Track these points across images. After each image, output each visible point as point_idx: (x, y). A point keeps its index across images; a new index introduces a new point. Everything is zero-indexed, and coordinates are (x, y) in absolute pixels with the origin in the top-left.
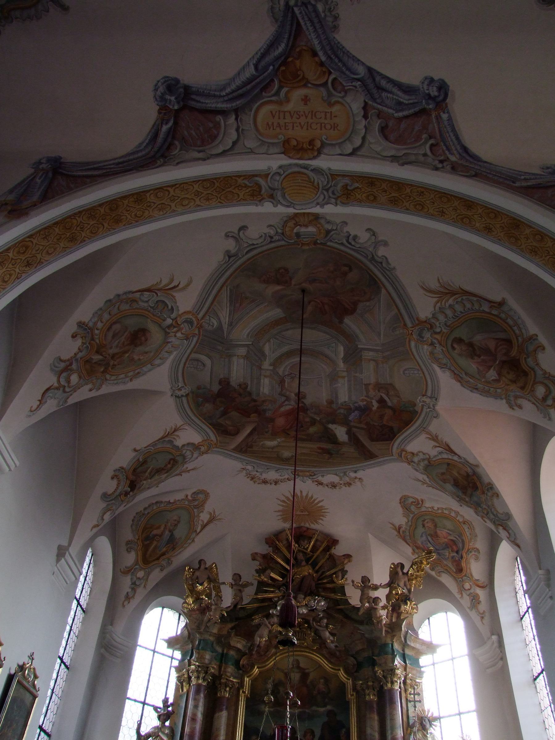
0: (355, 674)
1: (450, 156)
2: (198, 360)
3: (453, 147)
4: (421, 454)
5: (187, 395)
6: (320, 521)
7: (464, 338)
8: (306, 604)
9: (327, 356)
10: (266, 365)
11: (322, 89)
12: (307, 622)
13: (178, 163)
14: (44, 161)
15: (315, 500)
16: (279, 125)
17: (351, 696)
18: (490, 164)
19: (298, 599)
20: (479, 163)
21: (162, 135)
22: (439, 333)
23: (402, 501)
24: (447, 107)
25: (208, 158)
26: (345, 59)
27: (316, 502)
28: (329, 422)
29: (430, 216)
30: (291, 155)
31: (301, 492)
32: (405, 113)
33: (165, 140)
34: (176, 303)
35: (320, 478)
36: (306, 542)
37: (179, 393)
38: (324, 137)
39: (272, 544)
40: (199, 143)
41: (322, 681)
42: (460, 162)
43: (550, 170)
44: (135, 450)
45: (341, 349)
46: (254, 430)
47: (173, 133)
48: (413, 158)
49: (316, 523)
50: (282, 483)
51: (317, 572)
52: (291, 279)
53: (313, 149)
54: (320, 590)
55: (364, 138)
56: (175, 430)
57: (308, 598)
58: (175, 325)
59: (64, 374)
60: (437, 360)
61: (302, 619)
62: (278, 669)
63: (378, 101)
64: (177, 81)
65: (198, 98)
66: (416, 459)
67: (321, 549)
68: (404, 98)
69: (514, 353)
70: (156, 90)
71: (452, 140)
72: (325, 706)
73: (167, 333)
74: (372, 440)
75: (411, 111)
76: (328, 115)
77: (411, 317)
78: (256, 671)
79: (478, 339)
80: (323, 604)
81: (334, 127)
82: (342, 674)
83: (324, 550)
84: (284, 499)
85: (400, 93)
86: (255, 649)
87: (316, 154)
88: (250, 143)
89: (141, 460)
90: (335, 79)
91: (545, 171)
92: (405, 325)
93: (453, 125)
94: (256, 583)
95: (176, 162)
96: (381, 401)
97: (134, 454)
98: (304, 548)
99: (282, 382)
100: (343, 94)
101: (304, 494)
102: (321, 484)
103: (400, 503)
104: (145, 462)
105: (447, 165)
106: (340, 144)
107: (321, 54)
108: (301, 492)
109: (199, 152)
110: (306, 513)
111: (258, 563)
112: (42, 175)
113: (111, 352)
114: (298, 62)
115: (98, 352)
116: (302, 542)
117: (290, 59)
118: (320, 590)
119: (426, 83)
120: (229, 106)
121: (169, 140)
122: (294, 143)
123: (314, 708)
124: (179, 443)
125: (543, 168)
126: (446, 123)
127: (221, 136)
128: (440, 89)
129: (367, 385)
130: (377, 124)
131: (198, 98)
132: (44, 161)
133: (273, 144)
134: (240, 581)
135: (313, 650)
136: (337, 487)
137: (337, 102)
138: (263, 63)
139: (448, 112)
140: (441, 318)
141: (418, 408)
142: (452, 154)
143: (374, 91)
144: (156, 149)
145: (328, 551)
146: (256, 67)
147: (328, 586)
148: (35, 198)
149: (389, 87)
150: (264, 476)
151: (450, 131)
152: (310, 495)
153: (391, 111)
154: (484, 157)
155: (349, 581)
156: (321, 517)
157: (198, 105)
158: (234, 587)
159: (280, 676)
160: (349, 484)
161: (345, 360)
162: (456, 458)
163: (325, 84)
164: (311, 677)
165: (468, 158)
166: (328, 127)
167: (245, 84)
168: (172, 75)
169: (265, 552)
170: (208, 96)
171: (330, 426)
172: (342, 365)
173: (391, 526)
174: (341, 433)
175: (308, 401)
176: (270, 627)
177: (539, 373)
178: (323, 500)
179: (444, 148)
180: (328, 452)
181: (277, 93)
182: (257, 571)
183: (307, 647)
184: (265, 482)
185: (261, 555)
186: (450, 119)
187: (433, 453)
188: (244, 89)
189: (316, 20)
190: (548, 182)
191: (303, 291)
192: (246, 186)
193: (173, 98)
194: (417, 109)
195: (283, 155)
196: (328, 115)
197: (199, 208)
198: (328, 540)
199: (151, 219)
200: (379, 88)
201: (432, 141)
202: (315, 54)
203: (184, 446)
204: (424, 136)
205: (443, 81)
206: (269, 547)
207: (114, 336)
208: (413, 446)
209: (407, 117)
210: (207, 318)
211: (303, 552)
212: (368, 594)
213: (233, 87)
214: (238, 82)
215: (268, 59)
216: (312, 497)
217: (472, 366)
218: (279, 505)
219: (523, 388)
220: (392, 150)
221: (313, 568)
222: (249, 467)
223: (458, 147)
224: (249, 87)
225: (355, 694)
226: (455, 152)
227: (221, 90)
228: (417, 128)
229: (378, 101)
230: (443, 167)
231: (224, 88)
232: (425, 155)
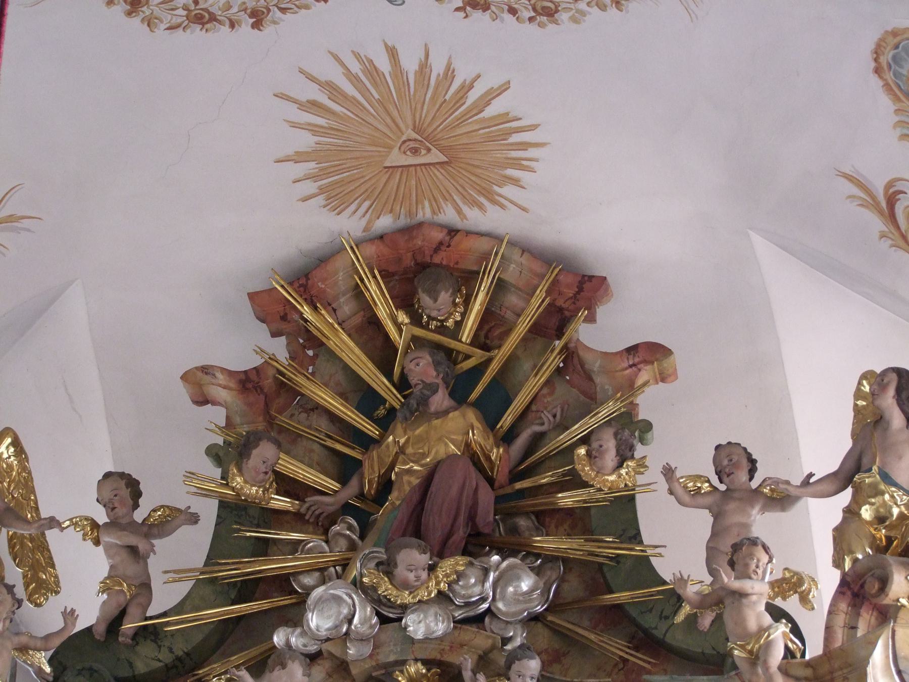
6: (508, 191)
8: (440, 593)
15: (467, 87)
19: (401, 571)
23: (883, 60)
27: (473, 96)
31: (392, 53)
36: (444, 297)
39: (284, 318)
49: (494, 202)
50: (288, 16)
51: (508, 438)
54: (523, 523)
57: (448, 566)
61: (426, 663)
67: (522, 328)
80: (525, 585)
83: (536, 330)
94: (209, 510)
98: (441, 329)
101: (410, 64)
103: (878, 71)
108: (392, 53)
110: (436, 156)
111: (218, 415)
116: (425, 299)
118: (523, 523)
134: (136, 506)
136: (564, 16)
145: (560, 334)
147: (567, 499)
152: (438, 66)
155: (654, 474)
156: (510, 172)
158: (106, 538)
169: (246, 361)
173: (856, 191)
178: (505, 87)
182: (215, 454)
185: (230, 373)
198: (555, 282)
206: (274, 334)
211: (437, 347)
212: (746, 526)
216: (449, 73)
218: (295, 125)
221: (491, 422)
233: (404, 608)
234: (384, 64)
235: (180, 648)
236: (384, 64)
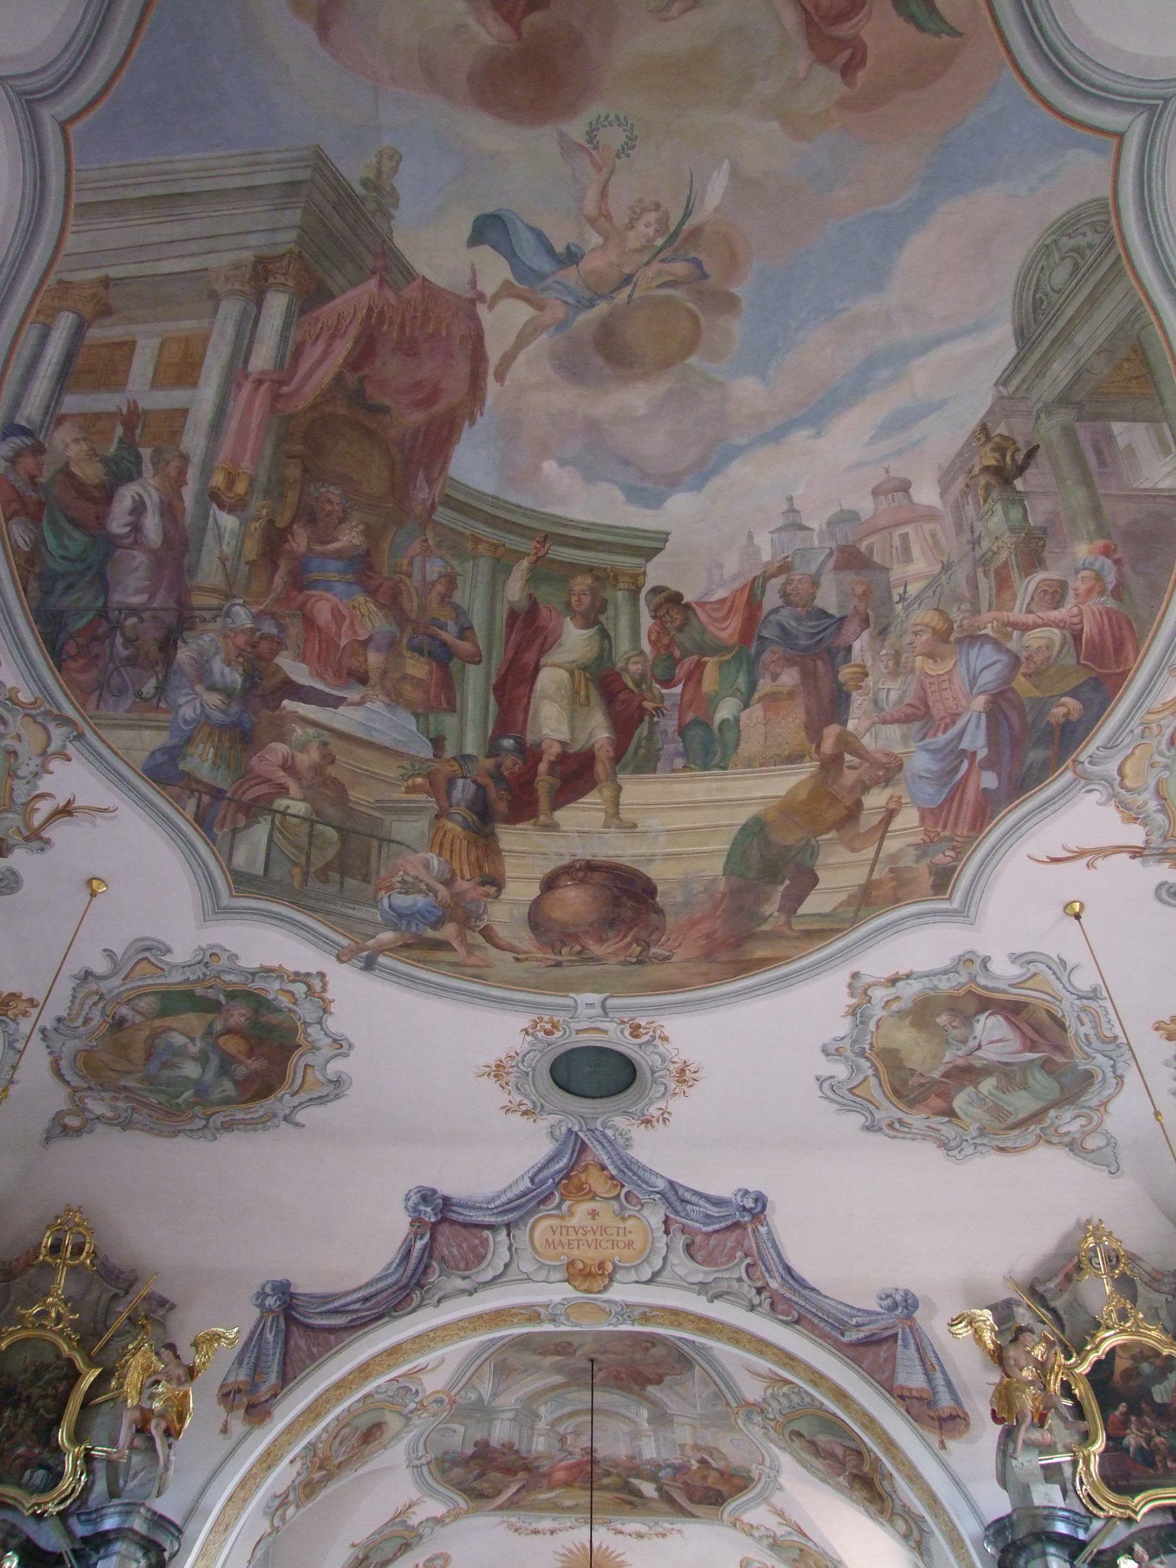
2: (447, 1429)
4: (762, 1529)
5: (428, 1463)
7: (804, 1432)
9: (623, 1416)
10: (541, 1425)
11: (613, 1202)
13: (439, 1301)
14: (268, 1290)
16: (561, 1243)
18: (819, 1294)
20: (805, 1292)
21: (416, 1253)
22: (772, 1420)
25: (476, 1290)
26: (641, 1173)
29: (749, 1351)
30: (576, 1284)
32: (717, 1227)
33: (420, 1260)
34: (422, 1384)
35: (619, 1527)
37: (418, 1463)
38: (616, 1259)
40: (462, 1265)
42: (782, 1291)
43: (889, 1301)
44: (353, 1545)
45: (645, 1413)
46: (523, 1487)
47: (430, 1249)
48: (724, 1286)
52: (575, 1351)
53: (603, 1275)
55: (665, 1259)
56: (410, 1506)
58: (422, 1406)
59: (279, 1513)
60: (772, 1441)
63: (683, 1214)
64: (434, 1192)
65: (460, 1210)
66: (756, 1533)
68: (713, 1211)
69: (866, 1468)
70: (407, 1199)
73: (408, 1419)
75: (723, 1225)
76: (621, 1231)
77: (735, 1398)
79: (822, 1439)
81: (629, 1245)
84: (563, 1551)
85: (707, 1205)
87: (607, 1281)
88: (527, 1266)
89: (360, 1556)
90: (629, 1192)
91: (884, 1303)
92: (728, 1404)
95: (436, 1298)
96: (702, 1462)
97: (352, 1550)
99: (563, 1439)
100: (639, 1207)
102: (621, 1532)
104: (366, 1557)
106: (636, 1267)
107: (611, 1168)
109: (464, 1278)
112: (272, 1321)
113: (337, 1462)
114: (583, 1177)
115: (321, 1468)
117: (573, 1173)
119: (740, 1194)
120: (499, 1219)
121: (425, 1260)
122: (580, 1265)
124: (414, 1521)
125: (881, 1299)
126: (765, 1237)
127: (489, 1256)
128: (756, 1200)
129: (682, 1446)
130: (680, 1241)
131: (460, 1210)
132: (268, 1290)
133: (555, 1267)
137: (631, 1216)
138: (541, 1176)
139: (767, 1225)
140: (774, 1404)
141: (755, 1474)
142: (772, 1277)
143: (677, 1204)
144: (409, 1273)
146: (532, 1180)
148: (273, 1378)
149: (695, 1199)
150: (534, 1526)
151: (769, 1245)
152: (604, 1546)
153: (697, 1225)
154: (811, 1280)
157: (461, 1219)
160: (664, 1535)
161: (649, 1421)
162: (810, 1544)
163: (617, 1197)
165: (791, 1282)
166: (621, 1245)
167: (518, 1197)
168: (429, 1184)
170: (474, 1208)
171: (632, 1480)
172: (646, 1425)
174: (648, 1489)
175: (598, 1455)
177: (897, 1502)
179: (763, 1269)
180: (631, 1503)
181: (559, 1207)
184: (535, 1532)
186: (769, 1232)
187: (780, 1531)
188: (518, 1202)
189: (604, 1141)
190: (886, 1329)
191: (592, 1361)
192: (522, 1314)
193: (429, 1209)
194: (729, 1222)
195: (567, 1284)
196: (621, 1231)
197: (462, 1338)
199: (405, 1361)
200: (683, 1201)
201: (749, 1260)
202: (603, 1168)
203: (421, 1523)
204: (739, 1254)
205: (760, 1193)
207: (341, 1443)
208: (750, 1517)
209: (716, 1231)
210: (463, 1393)
213: (504, 1199)
214: (510, 1195)
215: (546, 1173)
216: (607, 1548)
217: (818, 1464)
219: (881, 1513)
220: (698, 1273)
222: (513, 1520)
223: (780, 1268)
224: (523, 1200)
226: (776, 1274)
227: (489, 1203)
228: (729, 1244)
229: (683, 1214)
231: (493, 1200)
232: (740, 1280)
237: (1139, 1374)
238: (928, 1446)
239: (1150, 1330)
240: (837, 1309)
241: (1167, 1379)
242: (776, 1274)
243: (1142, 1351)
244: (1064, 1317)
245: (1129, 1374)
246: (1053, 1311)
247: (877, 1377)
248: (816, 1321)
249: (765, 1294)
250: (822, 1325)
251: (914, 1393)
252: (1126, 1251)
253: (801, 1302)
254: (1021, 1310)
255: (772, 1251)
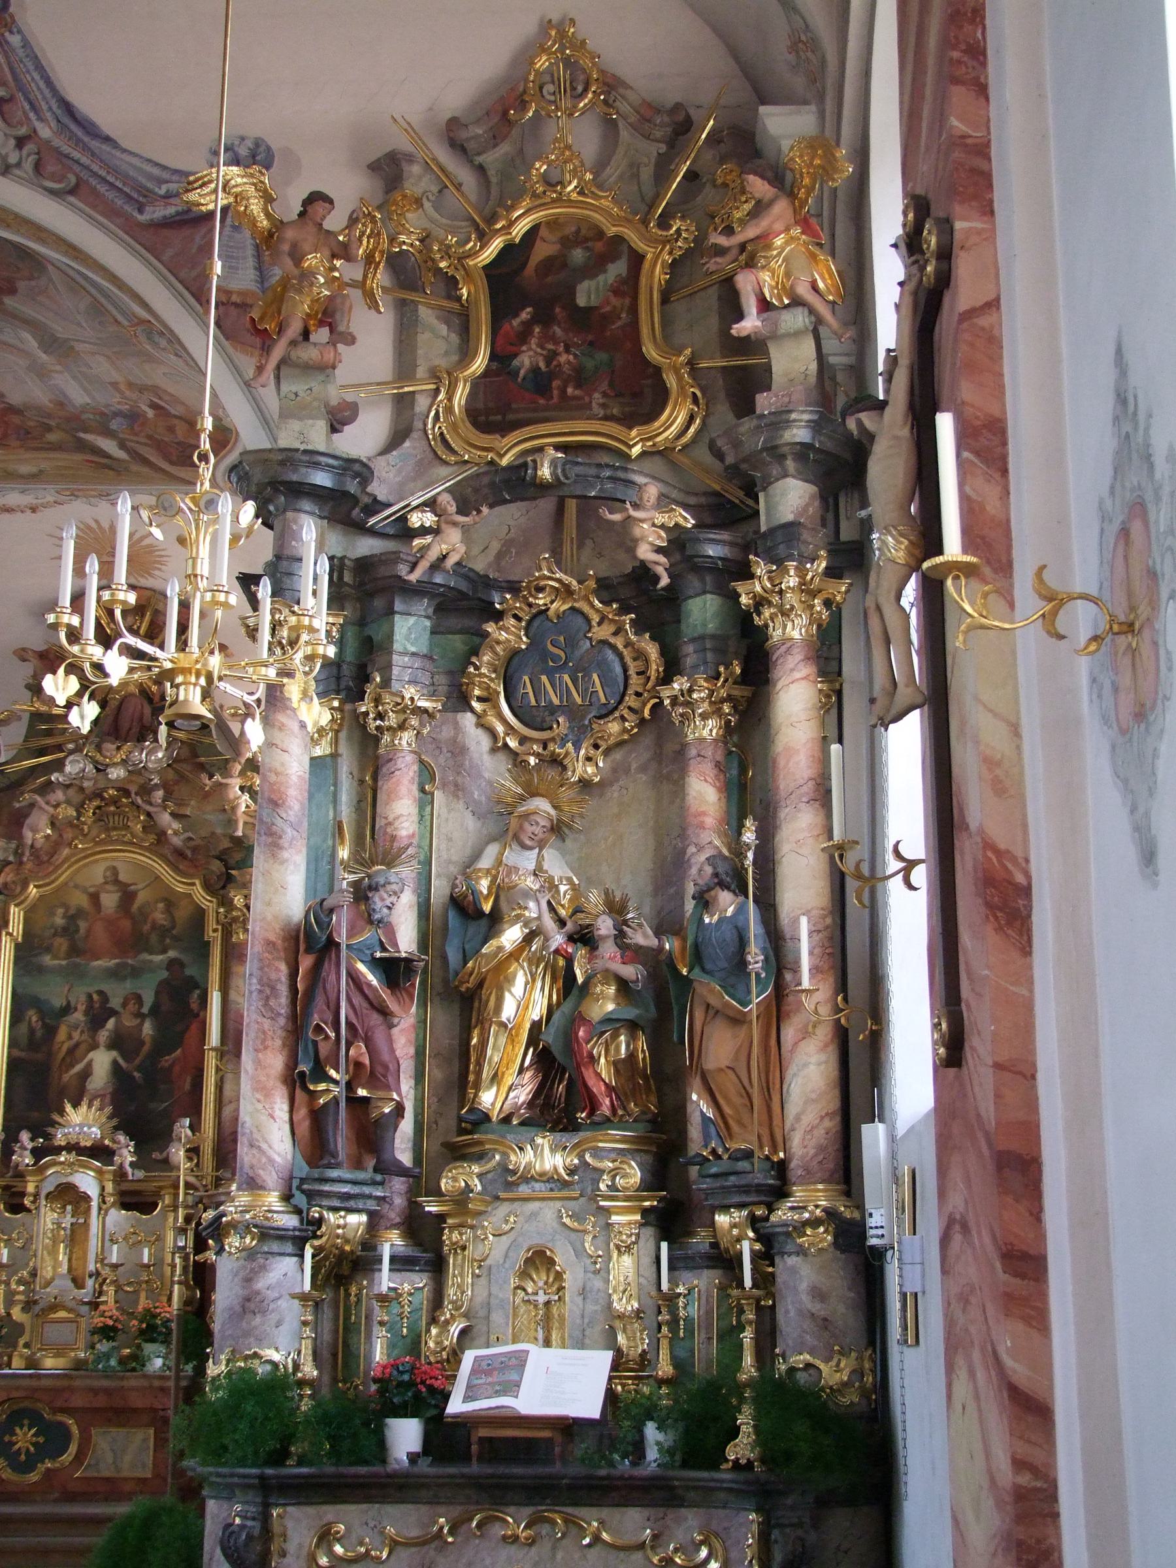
0: (221, 892)
1: (39, 125)
3: (43, 103)
6: (157, 572)
12: (126, 793)
17: (213, 933)
20: (95, 144)
24: (14, 21)
28: (78, 431)
31: (96, 521)
41: (161, 905)
42: (57, 142)
61: (118, 789)
62: (76, 886)
71: (39, 89)
72: (164, 951)
74: (172, 463)
78: (32, 891)
82: (199, 894)
86: (27, 853)
93: (36, 57)
105: (29, 155)
108: (96, 521)
123: (146, 956)
126: (21, 53)
135: (141, 847)
139: (19, 32)
142: (41, 119)
151: (31, 68)
159: (80, 900)
164: (142, 897)
165: (73, 127)
171: (82, 435)
176: (51, 810)
179: (27, 107)
183: (132, 843)
186: (26, 44)
223: (54, 104)
225: (220, 927)
226: (48, 115)
230: (18, 165)
233: (107, 766)
234: (94, 525)
235: (13, 778)
236: (94, 525)
237: (564, 265)
238: (237, 370)
239: (600, 198)
240: (140, 170)
241: (605, 271)
242: (48, 115)
243: (578, 231)
244: (494, 180)
245: (548, 265)
246: (481, 169)
247: (182, 275)
248: (102, 188)
249: (30, 147)
250: (111, 195)
251: (234, 298)
252: (602, 72)
253: (84, 160)
254: (416, 169)
255: (37, 77)
